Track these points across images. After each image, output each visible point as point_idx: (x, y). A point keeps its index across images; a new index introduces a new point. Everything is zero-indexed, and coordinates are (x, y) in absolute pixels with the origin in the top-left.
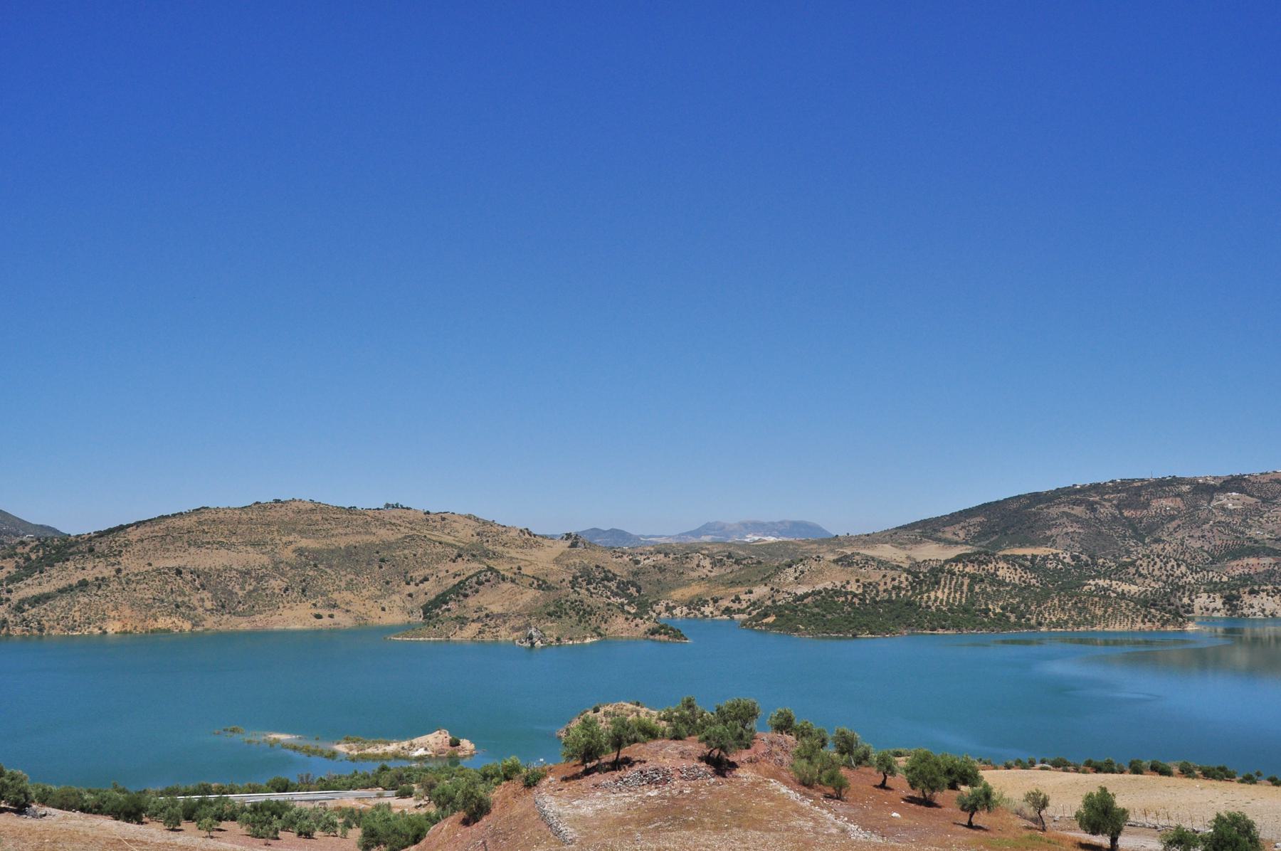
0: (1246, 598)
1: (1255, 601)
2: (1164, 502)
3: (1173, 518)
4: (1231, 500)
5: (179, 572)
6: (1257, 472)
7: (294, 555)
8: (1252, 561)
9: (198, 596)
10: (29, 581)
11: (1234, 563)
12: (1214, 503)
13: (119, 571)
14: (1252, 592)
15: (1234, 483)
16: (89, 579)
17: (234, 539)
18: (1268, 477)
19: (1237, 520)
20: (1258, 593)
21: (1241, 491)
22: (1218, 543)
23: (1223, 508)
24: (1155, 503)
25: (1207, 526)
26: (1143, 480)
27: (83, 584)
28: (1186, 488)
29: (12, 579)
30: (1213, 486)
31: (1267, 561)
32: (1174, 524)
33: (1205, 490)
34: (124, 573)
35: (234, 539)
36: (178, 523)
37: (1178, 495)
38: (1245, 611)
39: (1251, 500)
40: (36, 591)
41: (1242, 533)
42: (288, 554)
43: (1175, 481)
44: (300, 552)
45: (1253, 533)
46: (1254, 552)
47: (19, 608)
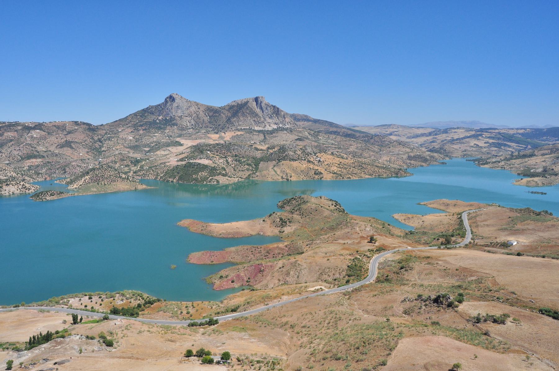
0: (5, 187)
1: (7, 188)
2: (9, 134)
3: (11, 141)
4: (35, 134)
6: (47, 121)
8: (34, 160)
11: (27, 161)
12: (29, 135)
14: (7, 185)
15: (39, 126)
18: (51, 124)
19: (35, 142)
20: (9, 185)
21: (41, 129)
22: (25, 152)
23: (32, 137)
24: (6, 134)
25: (22, 145)
26: (4, 123)
28: (20, 128)
30: (31, 127)
31: (39, 160)
32: (11, 143)
33: (27, 128)
37: (16, 131)
38: (3, 192)
39: (43, 133)
41: (35, 148)
43: (17, 124)
45: (41, 148)
46: (35, 157)
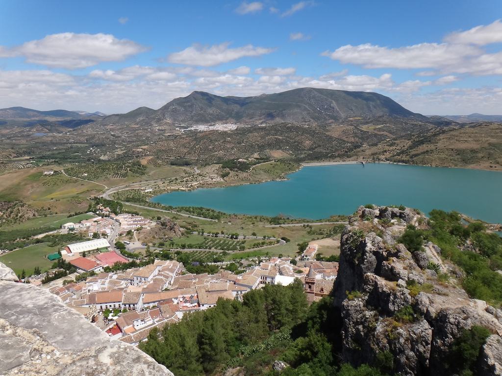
5: (452, 150)
7: (488, 145)
9: (457, 157)
10: (414, 149)
13: (436, 148)
16: (429, 150)
17: (470, 139)
27: (427, 151)
29: (411, 148)
34: (438, 148)
35: (470, 139)
36: (452, 133)
40: (416, 152)
42: (486, 145)
44: (490, 144)
47: (411, 157)
